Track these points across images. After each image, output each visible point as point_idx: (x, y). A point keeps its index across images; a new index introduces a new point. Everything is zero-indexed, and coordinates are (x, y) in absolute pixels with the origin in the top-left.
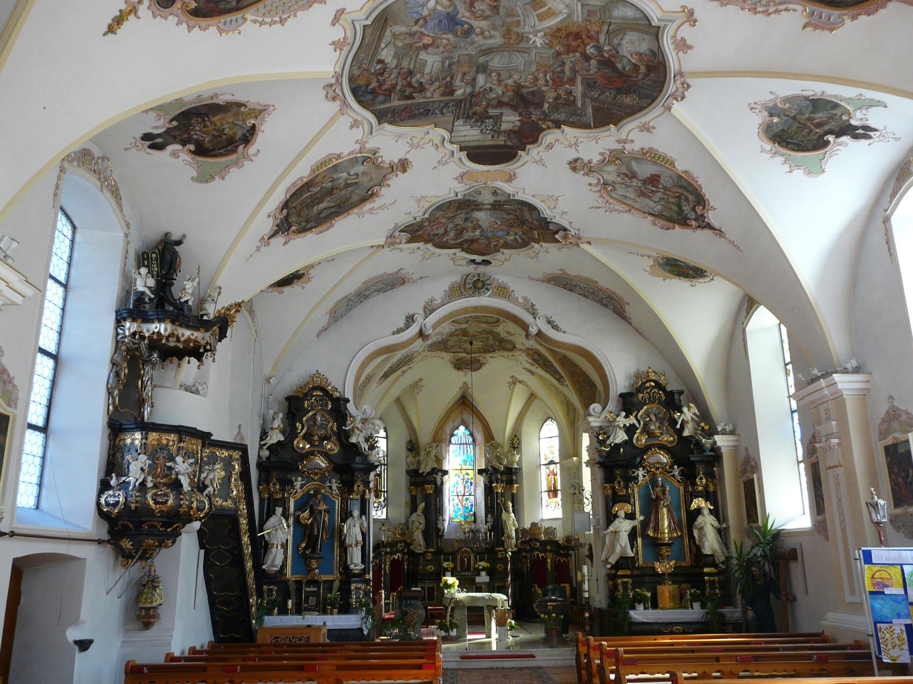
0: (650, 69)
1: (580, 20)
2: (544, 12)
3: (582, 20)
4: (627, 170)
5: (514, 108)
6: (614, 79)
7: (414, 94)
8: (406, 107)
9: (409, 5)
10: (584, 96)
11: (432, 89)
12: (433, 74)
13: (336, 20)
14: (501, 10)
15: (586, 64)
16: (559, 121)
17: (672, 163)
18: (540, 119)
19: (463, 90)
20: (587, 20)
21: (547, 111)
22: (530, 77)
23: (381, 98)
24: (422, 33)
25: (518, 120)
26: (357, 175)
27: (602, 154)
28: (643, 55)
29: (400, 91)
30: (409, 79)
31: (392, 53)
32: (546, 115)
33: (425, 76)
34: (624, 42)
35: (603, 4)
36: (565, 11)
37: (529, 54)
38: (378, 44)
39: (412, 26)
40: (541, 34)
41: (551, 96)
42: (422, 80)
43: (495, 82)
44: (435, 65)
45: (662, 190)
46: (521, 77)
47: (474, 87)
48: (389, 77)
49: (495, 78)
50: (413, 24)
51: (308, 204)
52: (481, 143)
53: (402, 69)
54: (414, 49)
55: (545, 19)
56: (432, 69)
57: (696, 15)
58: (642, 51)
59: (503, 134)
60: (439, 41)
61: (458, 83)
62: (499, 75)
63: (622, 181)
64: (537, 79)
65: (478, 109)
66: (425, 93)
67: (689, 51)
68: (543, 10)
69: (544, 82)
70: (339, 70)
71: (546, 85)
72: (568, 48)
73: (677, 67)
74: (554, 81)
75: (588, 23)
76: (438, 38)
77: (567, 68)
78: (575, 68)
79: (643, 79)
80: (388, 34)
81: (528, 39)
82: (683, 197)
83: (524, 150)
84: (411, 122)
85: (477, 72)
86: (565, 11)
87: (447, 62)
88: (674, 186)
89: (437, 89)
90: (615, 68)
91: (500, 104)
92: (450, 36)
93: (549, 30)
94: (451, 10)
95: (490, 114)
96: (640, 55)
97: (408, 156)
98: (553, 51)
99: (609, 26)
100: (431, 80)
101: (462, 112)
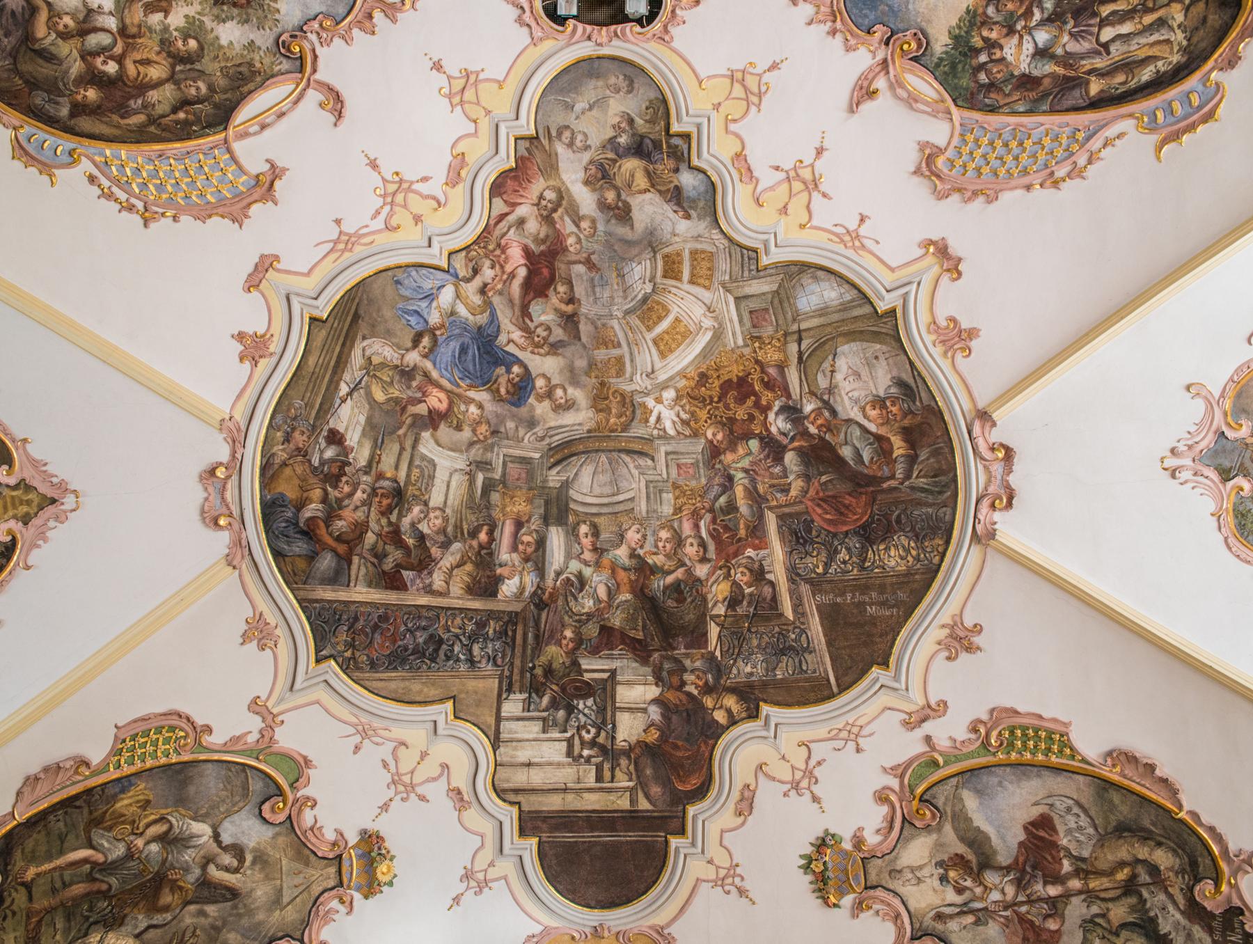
0: (909, 435)
1: (740, 342)
2: (666, 332)
3: (744, 340)
4: (962, 839)
5: (640, 651)
6: (848, 500)
7: (405, 574)
8: (385, 616)
9: (403, 292)
10: (794, 574)
11: (448, 560)
12: (448, 511)
13: (253, 283)
14: (582, 327)
15: (777, 470)
16: (751, 686)
17: (1066, 744)
18: (708, 689)
19: (516, 580)
20: (754, 338)
21: (718, 653)
22: (664, 534)
23: (326, 562)
24: (426, 375)
25: (656, 701)
26: (237, 850)
27: (881, 797)
28: (888, 404)
29: (373, 550)
30: (393, 518)
31: (362, 419)
32: (717, 669)
33: (432, 515)
34: (839, 377)
35: (775, 287)
36: (708, 323)
37: (653, 459)
38: (334, 384)
39: (407, 350)
40: (669, 395)
41: (719, 591)
42: (424, 528)
43: (587, 556)
44: (454, 484)
45: (1075, 884)
46: (644, 537)
47: (541, 571)
48: (351, 495)
49: (587, 542)
50: (410, 344)
51: (78, 901)
52: (572, 802)
53: (380, 476)
54: (409, 421)
55: (671, 351)
56: (447, 495)
57: (955, 248)
58: (882, 394)
59: (624, 762)
60: (463, 408)
61: (504, 556)
62: (596, 531)
63: (958, 899)
64: (679, 541)
65: (554, 653)
66: (430, 574)
67: (974, 344)
68: (664, 325)
69: (695, 548)
70: (240, 415)
71: (704, 560)
72: (731, 432)
73: (967, 405)
74: (715, 536)
75: (757, 345)
76: (459, 396)
77: (739, 491)
78: (755, 489)
79: (908, 476)
80: (356, 358)
81: (647, 412)
82: (1144, 877)
83: (682, 831)
84: (395, 680)
85: (546, 520)
86: (708, 323)
87: (480, 477)
88: (1102, 840)
89: (458, 566)
90: (838, 463)
91: (608, 638)
92: (482, 396)
93: (682, 383)
94: (483, 319)
95: (587, 676)
96: (879, 402)
97: (382, 826)
98: (700, 445)
99: (800, 341)
100: (443, 531)
101: (518, 662)
